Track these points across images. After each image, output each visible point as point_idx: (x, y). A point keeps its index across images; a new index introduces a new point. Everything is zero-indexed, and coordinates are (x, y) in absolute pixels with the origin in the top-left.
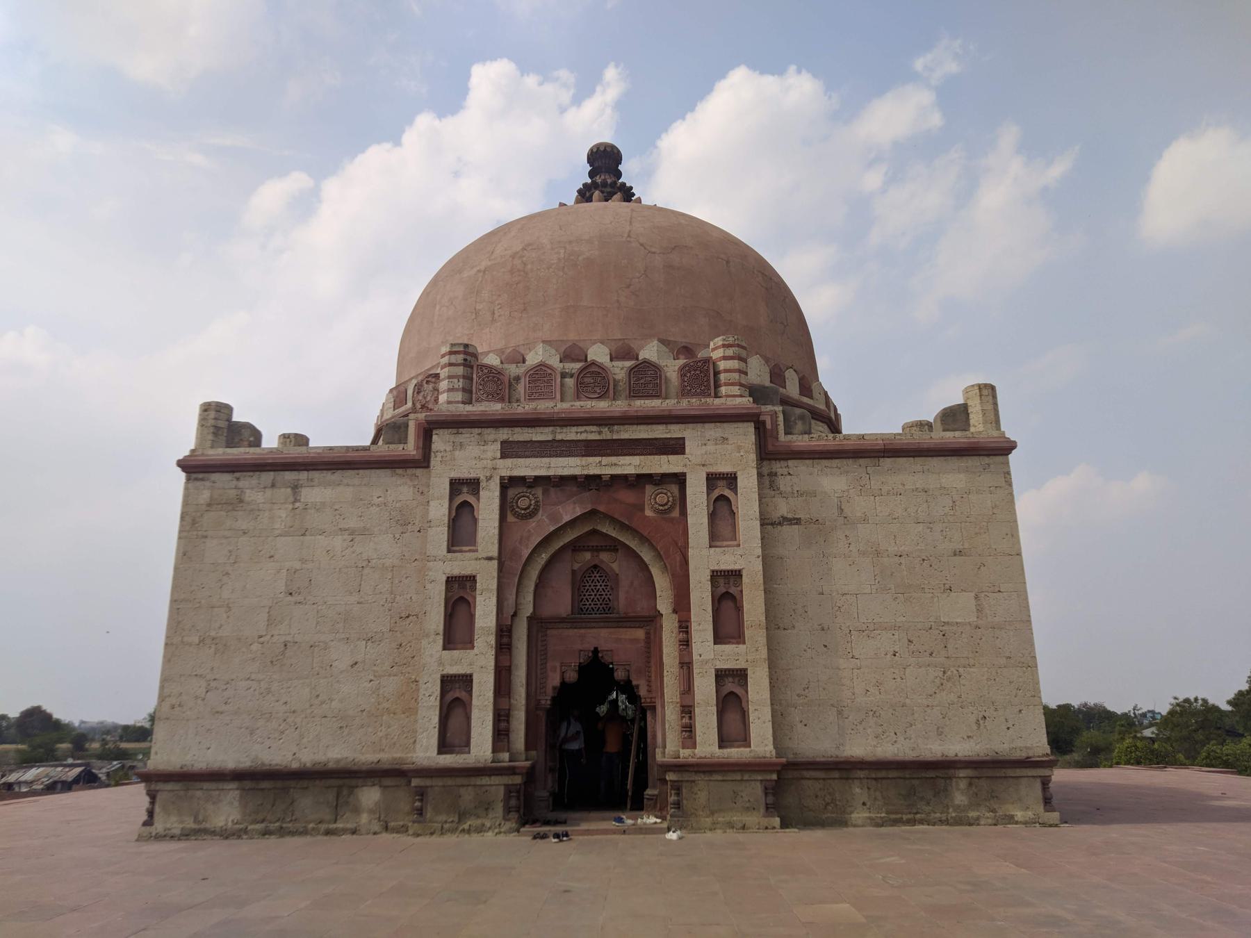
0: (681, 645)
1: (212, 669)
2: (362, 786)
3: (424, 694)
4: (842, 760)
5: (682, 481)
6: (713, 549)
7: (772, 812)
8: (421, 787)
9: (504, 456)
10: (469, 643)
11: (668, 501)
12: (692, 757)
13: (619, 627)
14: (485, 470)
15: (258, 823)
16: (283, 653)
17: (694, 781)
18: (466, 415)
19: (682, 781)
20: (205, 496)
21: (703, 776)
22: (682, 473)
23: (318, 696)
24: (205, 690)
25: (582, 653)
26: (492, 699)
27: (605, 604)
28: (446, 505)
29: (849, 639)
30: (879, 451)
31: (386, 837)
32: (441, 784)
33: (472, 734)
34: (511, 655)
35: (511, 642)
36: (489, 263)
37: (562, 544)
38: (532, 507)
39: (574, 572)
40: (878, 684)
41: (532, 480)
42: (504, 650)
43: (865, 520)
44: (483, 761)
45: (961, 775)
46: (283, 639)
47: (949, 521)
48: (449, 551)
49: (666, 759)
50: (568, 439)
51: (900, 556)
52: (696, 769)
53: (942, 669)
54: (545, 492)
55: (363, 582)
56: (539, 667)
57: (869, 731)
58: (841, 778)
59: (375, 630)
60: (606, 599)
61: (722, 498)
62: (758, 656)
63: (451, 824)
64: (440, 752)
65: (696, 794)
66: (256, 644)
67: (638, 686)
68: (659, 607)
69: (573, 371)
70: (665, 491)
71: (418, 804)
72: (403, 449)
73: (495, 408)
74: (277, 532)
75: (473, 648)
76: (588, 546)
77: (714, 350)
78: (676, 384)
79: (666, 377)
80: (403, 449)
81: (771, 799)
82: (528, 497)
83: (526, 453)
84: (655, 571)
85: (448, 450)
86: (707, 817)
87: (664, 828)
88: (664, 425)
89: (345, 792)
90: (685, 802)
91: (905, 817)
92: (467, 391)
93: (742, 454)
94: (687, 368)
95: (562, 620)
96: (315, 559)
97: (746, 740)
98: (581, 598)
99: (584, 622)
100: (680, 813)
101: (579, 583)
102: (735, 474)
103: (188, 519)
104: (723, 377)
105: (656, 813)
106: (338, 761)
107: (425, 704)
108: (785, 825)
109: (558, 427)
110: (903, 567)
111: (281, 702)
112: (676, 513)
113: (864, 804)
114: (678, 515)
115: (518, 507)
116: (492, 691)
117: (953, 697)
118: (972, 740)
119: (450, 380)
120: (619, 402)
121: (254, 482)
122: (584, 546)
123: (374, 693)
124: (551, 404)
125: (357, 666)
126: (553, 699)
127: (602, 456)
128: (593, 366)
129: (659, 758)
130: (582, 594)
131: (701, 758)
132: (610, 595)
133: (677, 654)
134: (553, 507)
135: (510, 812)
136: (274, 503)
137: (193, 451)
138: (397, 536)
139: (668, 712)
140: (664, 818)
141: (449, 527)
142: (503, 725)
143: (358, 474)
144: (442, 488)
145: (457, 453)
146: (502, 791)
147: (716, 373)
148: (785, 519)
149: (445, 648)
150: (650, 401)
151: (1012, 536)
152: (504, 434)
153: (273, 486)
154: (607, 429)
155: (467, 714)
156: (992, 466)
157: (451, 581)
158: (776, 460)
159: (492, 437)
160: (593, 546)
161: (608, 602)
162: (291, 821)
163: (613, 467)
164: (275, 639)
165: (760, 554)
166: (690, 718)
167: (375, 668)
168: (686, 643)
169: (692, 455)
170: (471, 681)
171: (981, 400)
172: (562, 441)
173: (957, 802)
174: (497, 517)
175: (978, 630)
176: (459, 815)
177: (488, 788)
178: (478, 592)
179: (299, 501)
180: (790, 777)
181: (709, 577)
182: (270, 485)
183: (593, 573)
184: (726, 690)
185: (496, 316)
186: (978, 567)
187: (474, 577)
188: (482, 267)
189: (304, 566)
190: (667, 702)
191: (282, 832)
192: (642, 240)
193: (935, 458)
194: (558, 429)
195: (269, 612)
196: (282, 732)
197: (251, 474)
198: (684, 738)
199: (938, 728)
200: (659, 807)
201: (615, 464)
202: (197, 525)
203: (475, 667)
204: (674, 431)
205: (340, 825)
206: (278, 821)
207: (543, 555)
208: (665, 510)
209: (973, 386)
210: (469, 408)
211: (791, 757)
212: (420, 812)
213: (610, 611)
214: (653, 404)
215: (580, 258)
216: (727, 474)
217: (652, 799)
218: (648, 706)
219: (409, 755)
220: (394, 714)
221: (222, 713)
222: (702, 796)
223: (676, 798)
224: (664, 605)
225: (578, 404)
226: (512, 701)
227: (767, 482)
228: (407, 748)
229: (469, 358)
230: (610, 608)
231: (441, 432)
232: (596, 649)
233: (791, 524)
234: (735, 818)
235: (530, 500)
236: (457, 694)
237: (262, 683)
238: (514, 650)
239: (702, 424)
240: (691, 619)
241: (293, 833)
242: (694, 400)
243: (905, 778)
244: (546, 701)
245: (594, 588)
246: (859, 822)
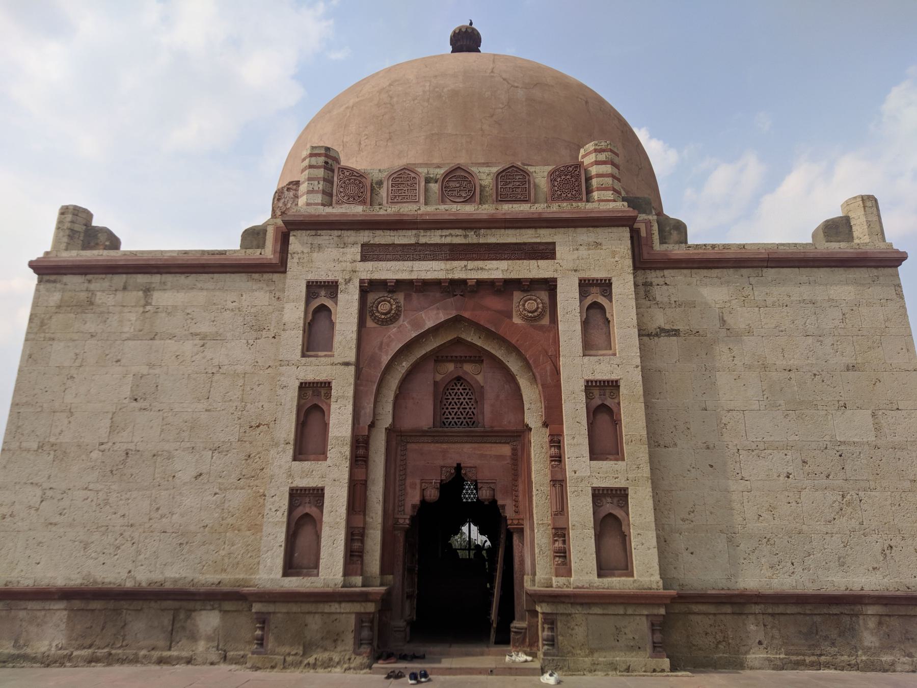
0: (552, 461)
1: (49, 477)
2: (201, 610)
3: (271, 509)
4: (736, 592)
5: (552, 287)
6: (587, 358)
7: (660, 652)
8: (263, 613)
9: (364, 259)
10: (322, 454)
11: (538, 308)
12: (567, 587)
13: (485, 443)
14: (344, 273)
15: (84, 648)
16: (124, 462)
17: (570, 614)
18: (324, 216)
19: (557, 614)
20: (56, 297)
21: (580, 609)
22: (553, 278)
23: (158, 509)
24: (39, 500)
25: (444, 469)
26: (344, 516)
27: (469, 418)
28: (302, 307)
29: (738, 460)
30: (762, 260)
31: (224, 667)
32: (284, 610)
33: (322, 554)
34: (367, 468)
35: (368, 455)
36: (357, 100)
37: (423, 352)
38: (393, 312)
39: (436, 384)
40: (771, 509)
41: (393, 284)
42: (360, 462)
43: (750, 332)
44: (332, 585)
45: (869, 612)
46: (125, 447)
47: (840, 335)
48: (303, 355)
49: (536, 588)
50: (432, 242)
51: (790, 370)
52: (572, 601)
53: (841, 493)
54: (408, 297)
55: (212, 389)
56: (397, 483)
57: (763, 560)
58: (733, 613)
59: (222, 440)
60: (470, 413)
61: (595, 306)
62: (639, 475)
63: (294, 658)
64: (285, 574)
65: (572, 629)
66: (97, 452)
67: (503, 506)
68: (526, 421)
69: (438, 176)
70: (534, 298)
71: (259, 632)
72: (261, 254)
73: (357, 210)
74: (124, 336)
75: (325, 459)
76: (452, 357)
77: (584, 156)
78: (545, 190)
79: (534, 182)
80: (261, 254)
81: (658, 637)
82: (389, 302)
83: (388, 256)
85: (305, 251)
86: (587, 656)
87: (535, 669)
88: (534, 230)
89: (182, 616)
90: (560, 638)
91: (808, 659)
92: (327, 194)
93: (617, 259)
94: (557, 173)
96: (163, 364)
97: (627, 568)
98: (443, 411)
99: (447, 436)
100: (555, 650)
101: (441, 395)
102: (609, 280)
103: (37, 321)
104: (594, 182)
105: (525, 649)
106: (175, 581)
107: (270, 520)
108: (674, 668)
109: (422, 231)
110: (793, 382)
111: (118, 515)
112: (546, 321)
113: (760, 643)
114: (548, 323)
115: (378, 312)
116: (345, 507)
117: (854, 523)
118: (878, 573)
119: (310, 182)
120: (485, 206)
121: (106, 284)
122: (447, 357)
123: (218, 507)
125: (201, 477)
126: (412, 518)
127: (468, 260)
128: (459, 170)
129: (528, 585)
130: (445, 407)
131: (578, 587)
132: (474, 408)
133: (548, 471)
134: (415, 312)
135: (361, 644)
136: (124, 306)
137: (47, 253)
138: (251, 342)
140: (534, 655)
141: (304, 331)
142: (356, 545)
143: (213, 278)
145: (315, 255)
146: (351, 622)
147: (588, 179)
149: (295, 459)
150: (519, 205)
151: (908, 350)
152: (366, 236)
153: (125, 288)
154: (473, 233)
155: (317, 532)
156: (881, 278)
157: (304, 387)
158: (650, 269)
160: (456, 357)
161: (472, 416)
162: (122, 646)
163: (480, 271)
164: (116, 447)
165: (639, 363)
166: (564, 542)
167: (220, 480)
168: (558, 459)
169: (563, 260)
170: (323, 495)
171: (865, 211)
172: (426, 245)
173: (866, 643)
174: (356, 320)
175: (877, 450)
176: (304, 646)
177: (338, 616)
178: (333, 399)
179: (150, 304)
180: (677, 611)
181: (584, 387)
182: (121, 289)
183: (456, 386)
184: (603, 513)
185: (362, 146)
186: (874, 382)
187: (329, 383)
188: (351, 103)
189: (151, 371)
190: (537, 524)
191: (110, 660)
192: (504, 76)
193: (822, 269)
194: (422, 233)
195: (112, 418)
196: (118, 548)
197: (104, 276)
198: (558, 565)
199: (839, 558)
200: (528, 642)
202: (44, 327)
203: (327, 479)
204: (544, 236)
205: (174, 653)
206: (107, 646)
207: (404, 364)
208: (538, 315)
209: (855, 198)
210: (329, 210)
212: (261, 642)
213: (474, 426)
214: (522, 209)
215: (445, 90)
216: (601, 280)
217: (521, 633)
218: (514, 528)
219: (253, 577)
220: (239, 530)
221: (56, 524)
222: (580, 632)
223: (550, 634)
224: (533, 417)
225: (442, 207)
226: (368, 519)
227: (643, 291)
228: (251, 568)
229: (330, 161)
230: (474, 422)
231: (299, 233)
232: (459, 465)
233: (669, 336)
234: (618, 659)
235: (391, 305)
236: (307, 510)
237: (100, 494)
238: (371, 463)
239: (573, 229)
240: (563, 432)
241: (122, 661)
242: (565, 204)
243: (805, 614)
244: (405, 520)
245: (457, 401)
246: (757, 664)
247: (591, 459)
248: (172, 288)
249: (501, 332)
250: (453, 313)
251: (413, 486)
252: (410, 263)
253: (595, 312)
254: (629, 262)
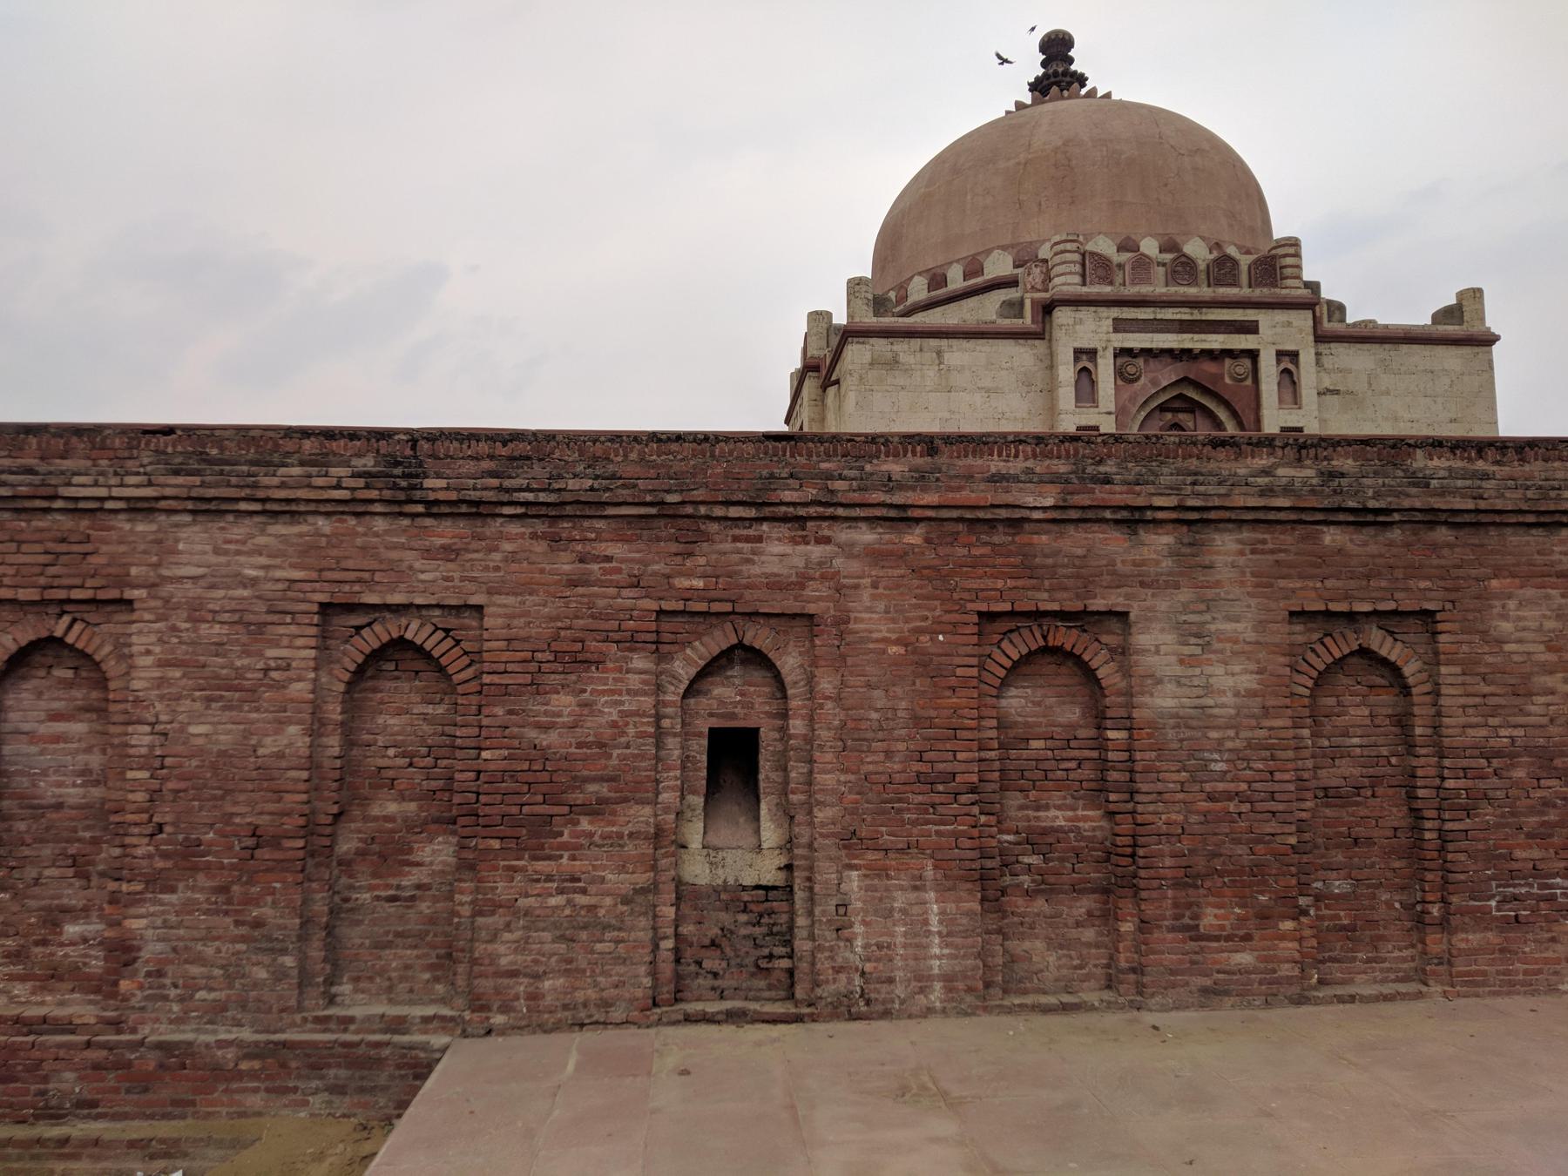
9: (1116, 330)
43: (1388, 393)
54: (1146, 362)
92: (1083, 276)
121: (906, 346)
124: (1151, 289)
144: (1065, 356)
148: (1328, 390)
152: (1115, 312)
159: (1105, 314)
194: (1158, 310)
210: (1085, 289)
225: (1173, 289)
248: (958, 350)
252: (1150, 335)
254: (1311, 338)
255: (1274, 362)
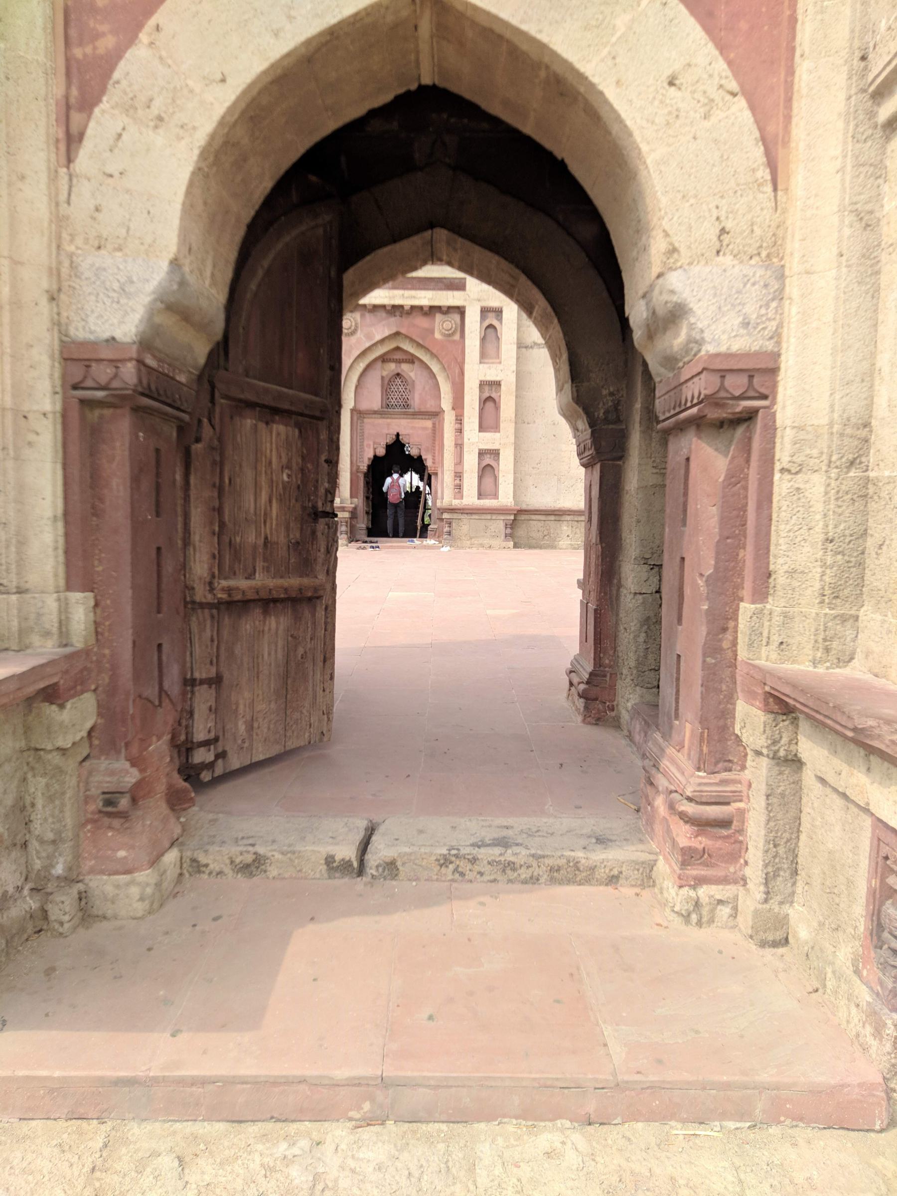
39: (383, 378)
54: (362, 316)
61: (491, 326)
81: (509, 531)
84: (441, 379)
95: (375, 412)
101: (387, 385)
108: (516, 546)
112: (457, 337)
126: (369, 466)
139: (446, 477)
140: (440, 542)
168: (460, 431)
184: (484, 463)
200: (438, 535)
201: (414, 297)
211: (524, 507)
224: (446, 404)
244: (364, 467)
246: (564, 547)
247: (480, 431)
249: (426, 345)
250: (394, 330)
251: (368, 446)
253: (490, 330)
255: (479, 319)
